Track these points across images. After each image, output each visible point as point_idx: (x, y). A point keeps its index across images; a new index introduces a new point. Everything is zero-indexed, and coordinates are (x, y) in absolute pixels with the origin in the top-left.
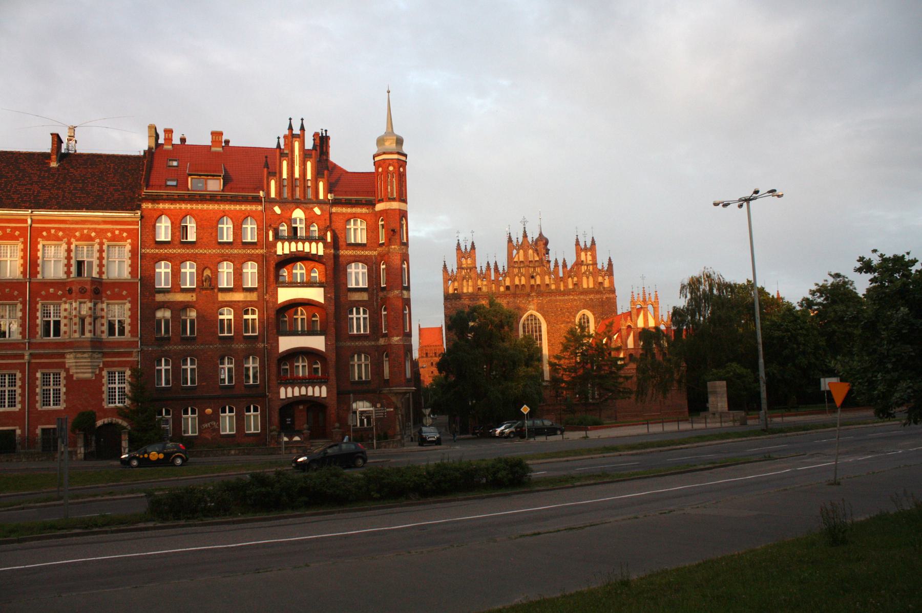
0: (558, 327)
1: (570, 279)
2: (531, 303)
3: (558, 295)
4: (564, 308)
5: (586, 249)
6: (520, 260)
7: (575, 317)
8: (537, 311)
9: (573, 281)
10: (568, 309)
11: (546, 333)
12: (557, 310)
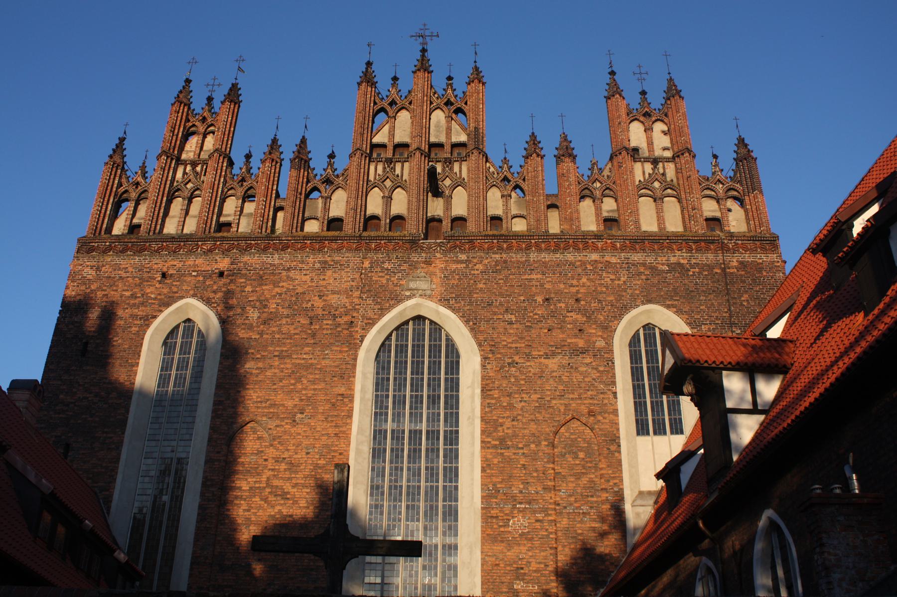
0: (533, 367)
1: (587, 203)
2: (420, 272)
3: (537, 246)
4: (558, 292)
5: (649, 129)
6: (397, 140)
7: (608, 330)
8: (444, 301)
9: (598, 210)
10: (577, 300)
11: (478, 391)
12: (531, 299)
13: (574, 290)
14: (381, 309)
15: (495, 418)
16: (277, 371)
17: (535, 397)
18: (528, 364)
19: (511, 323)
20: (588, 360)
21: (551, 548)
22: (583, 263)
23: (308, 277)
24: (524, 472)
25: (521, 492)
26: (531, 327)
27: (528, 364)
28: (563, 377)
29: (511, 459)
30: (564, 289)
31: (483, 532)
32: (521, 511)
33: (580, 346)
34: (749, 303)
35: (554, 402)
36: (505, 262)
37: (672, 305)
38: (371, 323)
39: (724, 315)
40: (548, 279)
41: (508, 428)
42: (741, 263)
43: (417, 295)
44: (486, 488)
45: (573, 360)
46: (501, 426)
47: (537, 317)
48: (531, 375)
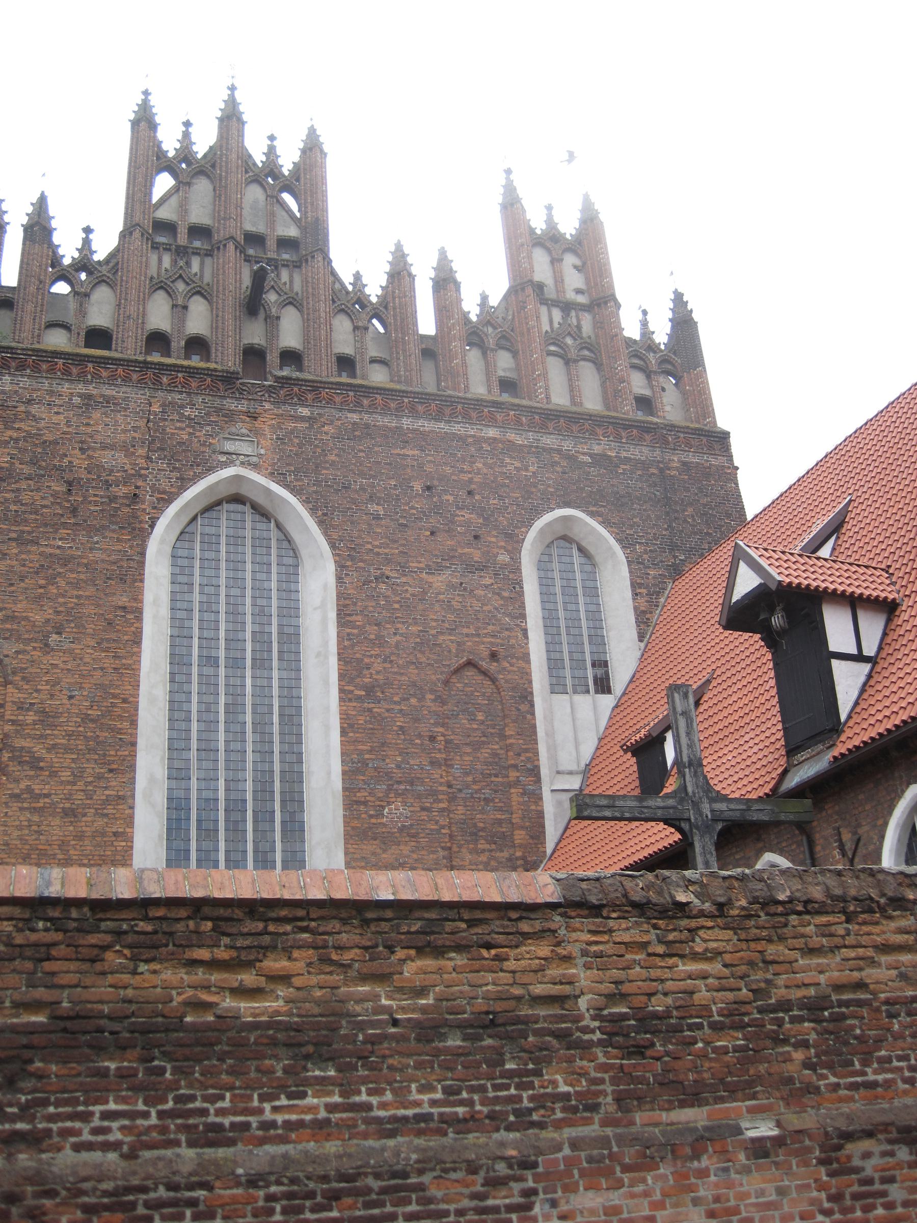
7: (514, 542)
11: (332, 615)
13: (466, 477)
14: (181, 479)
15: (358, 656)
16: (14, 563)
17: (414, 629)
18: (404, 579)
19: (377, 517)
20: (487, 581)
21: (443, 848)
22: (478, 440)
23: (61, 417)
24: (403, 737)
25: (398, 767)
26: (406, 526)
27: (404, 579)
28: (454, 603)
29: (383, 719)
30: (452, 474)
31: (346, 824)
32: (400, 795)
33: (476, 559)
34: (694, 520)
35: (441, 638)
36: (367, 426)
37: (597, 512)
38: (169, 500)
39: (664, 533)
40: (429, 458)
41: (378, 672)
42: (684, 464)
43: (238, 462)
44: (348, 759)
45: (467, 580)
46: (368, 668)
47: (414, 512)
48: (408, 596)
